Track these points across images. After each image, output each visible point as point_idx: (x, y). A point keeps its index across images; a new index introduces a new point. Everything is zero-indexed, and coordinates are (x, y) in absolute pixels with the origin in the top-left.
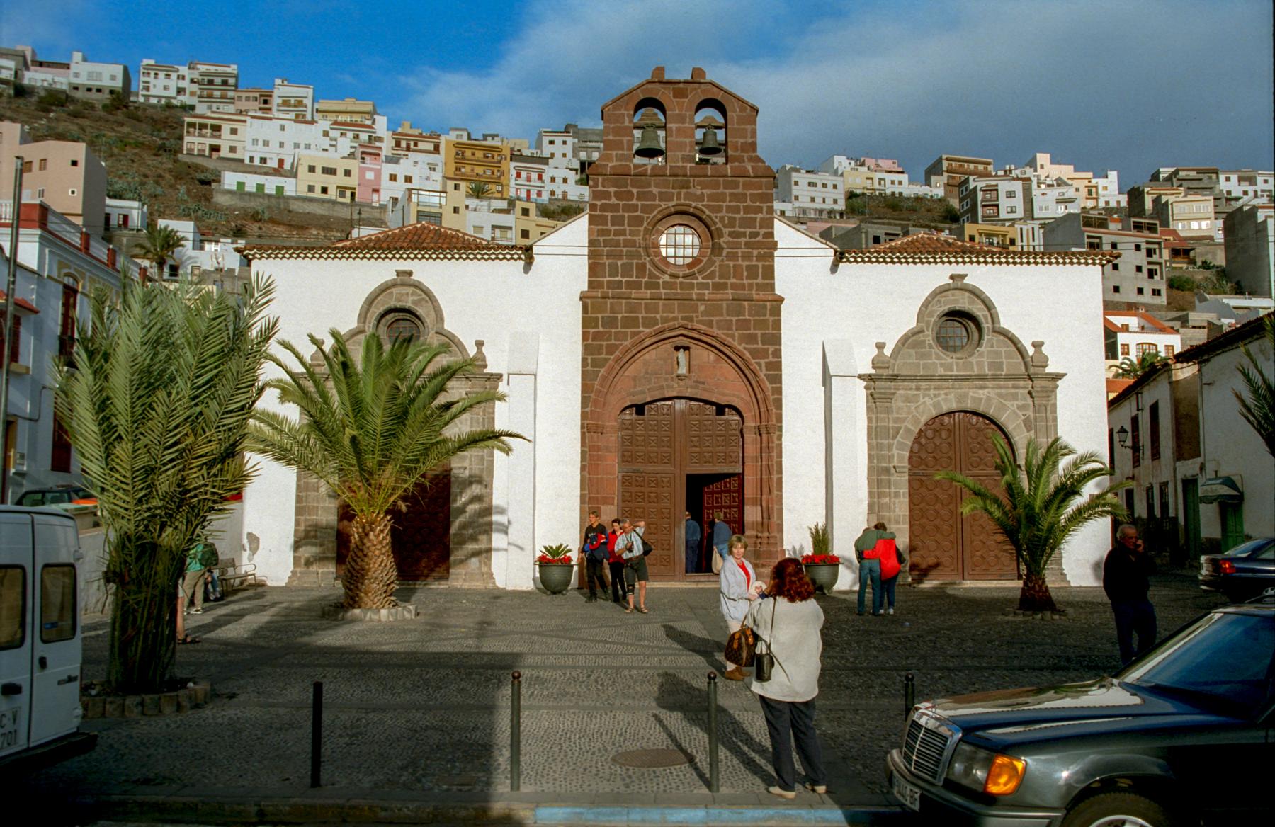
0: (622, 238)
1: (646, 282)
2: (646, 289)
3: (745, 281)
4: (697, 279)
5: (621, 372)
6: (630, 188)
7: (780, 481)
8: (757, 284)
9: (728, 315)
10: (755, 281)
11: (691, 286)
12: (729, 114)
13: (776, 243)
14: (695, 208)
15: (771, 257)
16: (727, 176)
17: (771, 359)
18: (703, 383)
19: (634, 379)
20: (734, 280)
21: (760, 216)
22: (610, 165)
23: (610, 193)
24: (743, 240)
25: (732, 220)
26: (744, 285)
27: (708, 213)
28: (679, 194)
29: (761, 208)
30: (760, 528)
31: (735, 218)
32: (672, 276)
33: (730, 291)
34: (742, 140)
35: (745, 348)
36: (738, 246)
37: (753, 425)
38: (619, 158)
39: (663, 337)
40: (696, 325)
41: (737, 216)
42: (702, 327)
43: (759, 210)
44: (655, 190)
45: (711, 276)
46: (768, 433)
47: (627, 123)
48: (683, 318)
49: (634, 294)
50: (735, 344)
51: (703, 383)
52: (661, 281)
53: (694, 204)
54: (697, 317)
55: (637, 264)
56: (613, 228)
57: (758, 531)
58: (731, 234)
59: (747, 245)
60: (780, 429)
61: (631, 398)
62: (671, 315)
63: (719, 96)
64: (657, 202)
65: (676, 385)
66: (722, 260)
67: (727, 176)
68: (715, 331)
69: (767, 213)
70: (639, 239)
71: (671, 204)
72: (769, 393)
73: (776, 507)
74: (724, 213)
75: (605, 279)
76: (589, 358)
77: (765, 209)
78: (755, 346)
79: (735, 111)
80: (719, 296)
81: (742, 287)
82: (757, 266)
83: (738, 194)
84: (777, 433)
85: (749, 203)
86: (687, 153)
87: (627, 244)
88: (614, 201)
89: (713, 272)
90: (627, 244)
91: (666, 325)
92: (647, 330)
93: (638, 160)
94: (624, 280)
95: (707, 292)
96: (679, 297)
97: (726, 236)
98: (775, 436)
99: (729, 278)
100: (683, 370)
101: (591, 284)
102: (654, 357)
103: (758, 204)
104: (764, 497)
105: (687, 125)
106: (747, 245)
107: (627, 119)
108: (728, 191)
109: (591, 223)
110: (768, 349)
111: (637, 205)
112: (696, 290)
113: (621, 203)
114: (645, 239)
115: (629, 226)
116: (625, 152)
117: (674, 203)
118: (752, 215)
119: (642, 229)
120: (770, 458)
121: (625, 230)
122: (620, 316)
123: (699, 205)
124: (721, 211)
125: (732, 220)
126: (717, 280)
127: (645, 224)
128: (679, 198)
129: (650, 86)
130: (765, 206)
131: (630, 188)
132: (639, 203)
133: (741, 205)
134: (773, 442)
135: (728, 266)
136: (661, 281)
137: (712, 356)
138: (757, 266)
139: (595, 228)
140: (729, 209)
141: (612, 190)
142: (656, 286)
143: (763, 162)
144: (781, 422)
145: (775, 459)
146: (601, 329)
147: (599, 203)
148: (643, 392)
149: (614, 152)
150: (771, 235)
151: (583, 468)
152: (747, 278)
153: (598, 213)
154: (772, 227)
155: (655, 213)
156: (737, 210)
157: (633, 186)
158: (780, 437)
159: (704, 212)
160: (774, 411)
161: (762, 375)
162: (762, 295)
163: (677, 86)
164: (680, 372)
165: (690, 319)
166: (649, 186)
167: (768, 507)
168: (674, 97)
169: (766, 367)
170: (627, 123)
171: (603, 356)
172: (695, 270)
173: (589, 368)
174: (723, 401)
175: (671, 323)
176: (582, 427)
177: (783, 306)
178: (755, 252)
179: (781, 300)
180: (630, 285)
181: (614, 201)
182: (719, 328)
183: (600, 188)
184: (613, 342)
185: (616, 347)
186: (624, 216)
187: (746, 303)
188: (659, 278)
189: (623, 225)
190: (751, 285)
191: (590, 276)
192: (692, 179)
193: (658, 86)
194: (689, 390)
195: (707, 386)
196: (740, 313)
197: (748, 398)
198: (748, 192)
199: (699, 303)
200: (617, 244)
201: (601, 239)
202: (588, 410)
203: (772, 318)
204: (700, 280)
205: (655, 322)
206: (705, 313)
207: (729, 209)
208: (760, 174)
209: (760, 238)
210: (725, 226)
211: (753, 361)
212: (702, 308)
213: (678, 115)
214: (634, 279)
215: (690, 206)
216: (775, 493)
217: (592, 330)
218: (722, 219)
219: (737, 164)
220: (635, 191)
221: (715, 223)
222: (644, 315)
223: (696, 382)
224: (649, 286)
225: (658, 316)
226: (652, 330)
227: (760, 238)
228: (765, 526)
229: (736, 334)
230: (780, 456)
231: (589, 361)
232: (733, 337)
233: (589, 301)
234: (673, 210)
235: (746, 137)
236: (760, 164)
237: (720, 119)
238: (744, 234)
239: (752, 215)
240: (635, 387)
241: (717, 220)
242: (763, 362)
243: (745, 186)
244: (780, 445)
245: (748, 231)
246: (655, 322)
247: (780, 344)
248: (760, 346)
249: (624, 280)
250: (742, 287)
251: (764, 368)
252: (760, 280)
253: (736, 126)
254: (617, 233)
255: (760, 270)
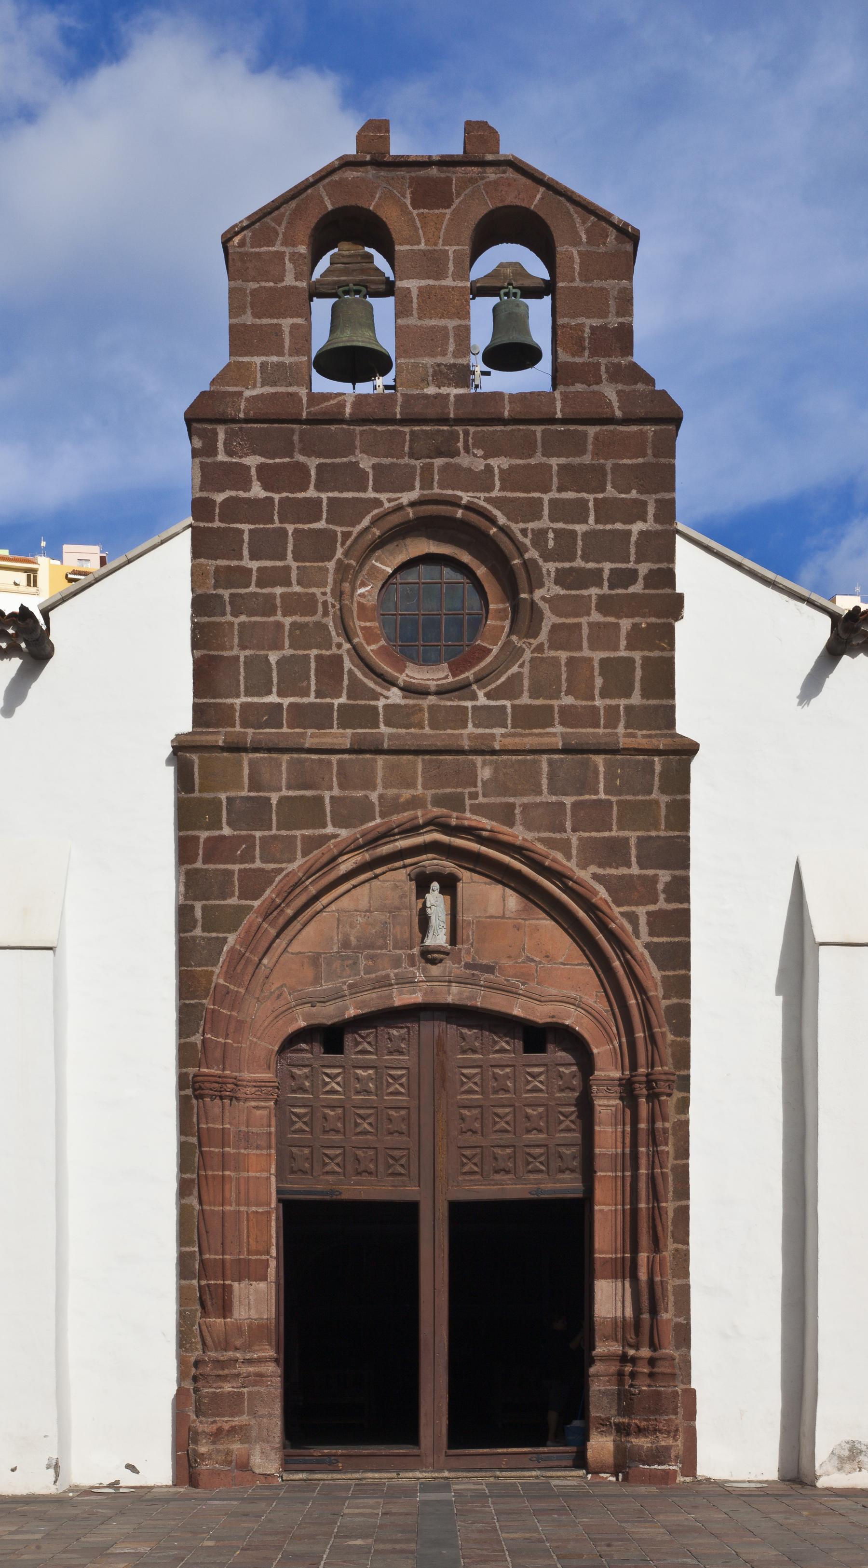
0: (279, 590)
1: (340, 706)
2: (342, 725)
3: (598, 702)
4: (474, 697)
5: (281, 943)
6: (301, 459)
7: (683, 1214)
8: (629, 709)
9: (552, 791)
10: (623, 702)
11: (459, 718)
12: (562, 249)
13: (681, 597)
14: (468, 508)
15: (668, 637)
16: (553, 421)
17: (662, 904)
18: (490, 969)
19: (315, 960)
20: (568, 700)
21: (637, 527)
22: (248, 393)
23: (249, 468)
24: (594, 591)
25: (566, 538)
26: (595, 709)
27: (502, 520)
28: (427, 470)
29: (644, 504)
30: (631, 1337)
31: (573, 533)
32: (409, 690)
33: (558, 729)
34: (596, 322)
35: (595, 877)
36: (580, 607)
37: (617, 1074)
38: (271, 375)
39: (385, 850)
40: (471, 819)
41: (580, 528)
42: (486, 823)
43: (637, 512)
44: (366, 463)
45: (510, 690)
46: (653, 1096)
47: (289, 280)
48: (438, 801)
49: (311, 737)
50: (571, 866)
51: (490, 969)
52: (381, 703)
53: (466, 497)
54: (473, 796)
55: (318, 658)
56: (254, 565)
57: (625, 1343)
58: (562, 578)
59: (605, 605)
60: (684, 1083)
61: (307, 1008)
62: (406, 794)
63: (536, 199)
64: (371, 494)
65: (420, 976)
66: (540, 648)
67: (553, 421)
68: (519, 834)
69: (657, 519)
70: (324, 593)
71: (406, 498)
72: (657, 992)
73: (672, 1283)
74: (545, 522)
75: (238, 702)
76: (198, 906)
77: (651, 510)
78: (623, 871)
79: (576, 242)
80: (529, 742)
81: (591, 717)
82: (631, 661)
83: (582, 467)
84: (677, 1095)
85: (610, 491)
86: (449, 360)
87: (292, 605)
88: (257, 491)
89: (519, 676)
90: (292, 605)
91: (397, 818)
92: (344, 833)
93: (322, 384)
94: (286, 701)
95: (498, 731)
96: (426, 744)
97: (549, 583)
98: (671, 1103)
99: (558, 697)
100: (438, 937)
101: (200, 714)
102: (364, 904)
103: (634, 494)
104: (643, 1257)
105: (449, 282)
106: (605, 605)
107: (289, 265)
108: (554, 462)
109: (197, 552)
110: (654, 879)
111: (319, 501)
112: (470, 729)
113: (276, 497)
114: (339, 594)
115: (296, 559)
116: (287, 360)
117: (414, 495)
118: (619, 526)
119: (331, 565)
120: (656, 1158)
121: (288, 569)
122: (274, 798)
123: (480, 499)
124: (537, 516)
125: (566, 538)
126: (525, 700)
127: (339, 553)
128: (427, 483)
129: (350, 174)
130: (651, 501)
131: (301, 459)
132: (324, 496)
133: (591, 497)
134: (665, 1119)
135: (556, 660)
136: (381, 703)
137: (513, 901)
138: (632, 661)
139: (211, 564)
140: (559, 510)
141: (253, 461)
142: (370, 717)
143: (650, 381)
144: (688, 1067)
145: (671, 1162)
146: (227, 831)
147: (220, 497)
148: (338, 995)
149: (258, 360)
150: (668, 577)
151: (184, 1189)
152: (603, 696)
153: (217, 524)
154: (671, 557)
155: (366, 522)
156: (577, 512)
157: (307, 451)
158: (684, 1105)
159: (493, 521)
160: (670, 1037)
161: (638, 947)
162: (641, 739)
163: (422, 173)
164: (429, 942)
165: (455, 802)
166: (350, 451)
167: (651, 1282)
168: (415, 206)
169: (649, 924)
170: (289, 280)
171: (233, 901)
172: (469, 674)
173: (198, 932)
174: (540, 1014)
175: (407, 815)
176: (183, 1082)
177: (696, 766)
178: (626, 624)
179: (690, 749)
180: (301, 716)
181: (257, 491)
182: (529, 827)
183: (221, 457)
184: (258, 864)
185: (266, 878)
186: (285, 531)
187: (599, 760)
188: (376, 696)
189: (283, 557)
190: (612, 712)
191: (197, 693)
192: (460, 429)
193: (370, 173)
194: (455, 989)
195: (497, 978)
196: (585, 784)
197: (601, 1006)
198: (609, 464)
199: (479, 760)
200: (268, 606)
201: (226, 594)
202: (197, 1039)
203: (664, 799)
204: (482, 701)
205: (364, 811)
206: (496, 786)
207: (559, 510)
208: (640, 412)
209: (637, 588)
210: (547, 556)
211: (617, 910)
212: (485, 773)
213: (424, 253)
214: (312, 699)
215: (454, 503)
216: (671, 1246)
217: (204, 835)
218: (539, 536)
219: (579, 387)
220: (313, 463)
221: (521, 550)
222: (336, 792)
223: (468, 966)
224: (349, 717)
225: (374, 797)
226: (357, 831)
227: (637, 588)
228: (646, 1330)
229: (574, 842)
230: (684, 1152)
231: (198, 913)
232: (564, 847)
233: (195, 757)
234: (411, 513)
235: (603, 314)
236: (640, 386)
237: (538, 269)
238: (595, 577)
239: (619, 526)
240: (317, 980)
241: (527, 542)
242: (641, 911)
243: (603, 447)
244: (683, 1128)
245: (607, 566)
246: (364, 811)
247: (687, 866)
248: (635, 870)
249: (286, 701)
250: (591, 717)
251: (644, 929)
252: (636, 699)
253: (578, 283)
254: (267, 578)
255: (638, 673)
